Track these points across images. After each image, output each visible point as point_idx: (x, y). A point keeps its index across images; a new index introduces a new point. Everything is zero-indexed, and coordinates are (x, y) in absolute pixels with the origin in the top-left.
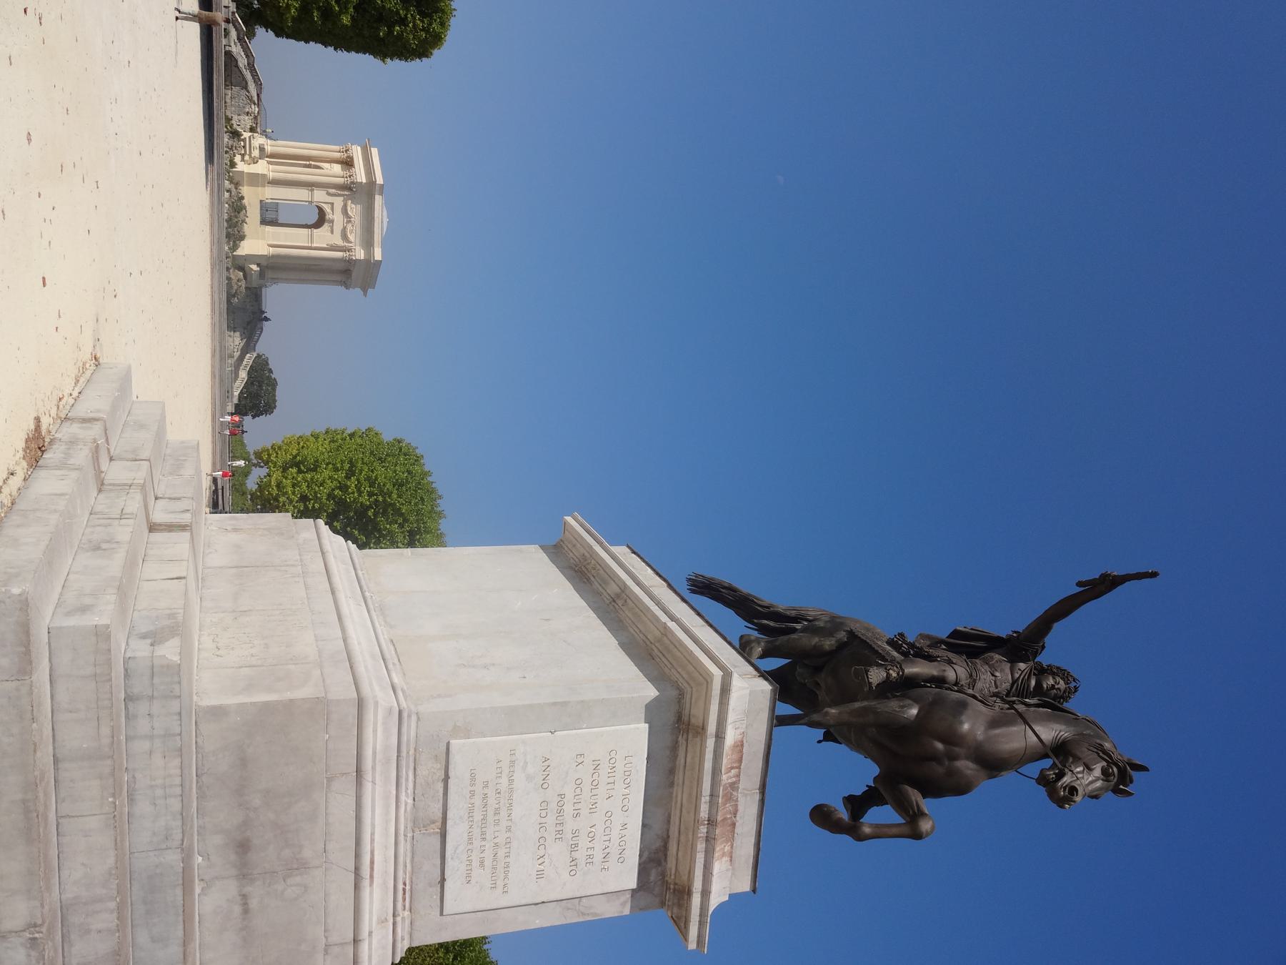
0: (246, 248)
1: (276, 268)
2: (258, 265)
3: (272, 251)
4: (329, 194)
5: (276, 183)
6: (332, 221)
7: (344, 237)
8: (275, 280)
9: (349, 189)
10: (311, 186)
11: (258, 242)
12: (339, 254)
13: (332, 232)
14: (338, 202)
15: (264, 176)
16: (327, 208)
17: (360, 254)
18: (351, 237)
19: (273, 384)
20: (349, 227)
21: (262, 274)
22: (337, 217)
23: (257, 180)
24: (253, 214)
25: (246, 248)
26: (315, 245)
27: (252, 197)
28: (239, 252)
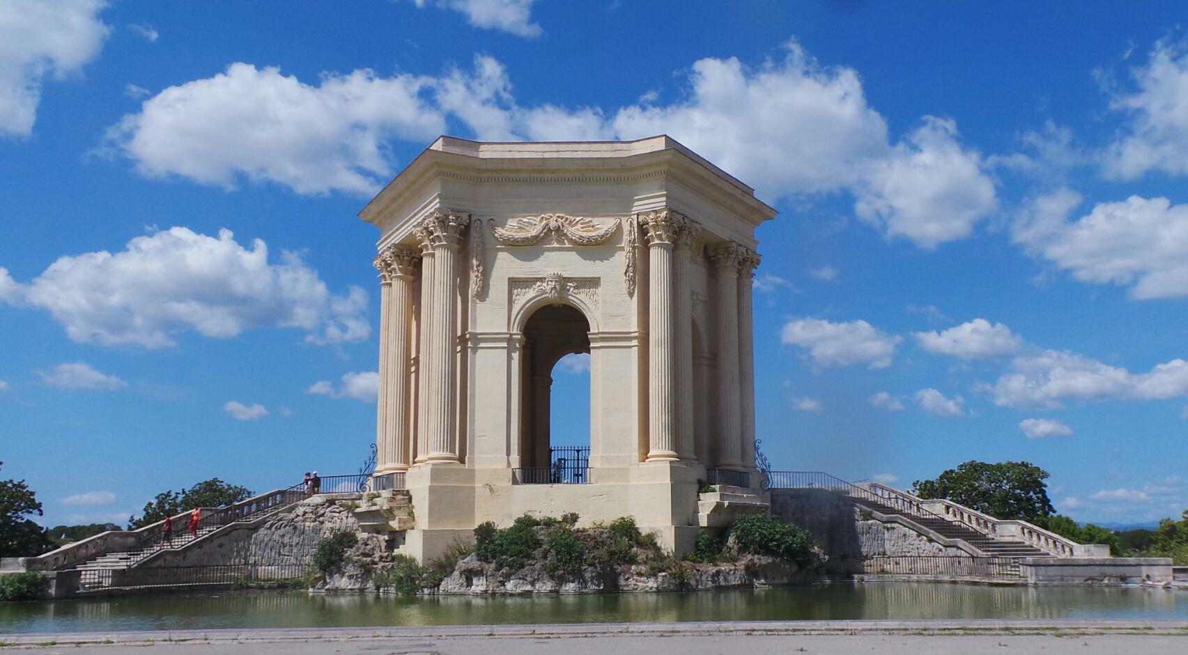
0: (656, 520)
1: (708, 438)
2: (703, 486)
3: (660, 447)
4: (483, 294)
6: (563, 281)
7: (599, 247)
8: (748, 446)
9: (468, 240)
10: (463, 343)
12: (658, 260)
13: (593, 283)
14: (506, 266)
15: (436, 473)
16: (525, 298)
18: (604, 225)
20: (577, 231)
21: (736, 479)
23: (451, 492)
24: (546, 502)
25: (656, 520)
26: (633, 326)
27: (509, 503)
28: (667, 542)
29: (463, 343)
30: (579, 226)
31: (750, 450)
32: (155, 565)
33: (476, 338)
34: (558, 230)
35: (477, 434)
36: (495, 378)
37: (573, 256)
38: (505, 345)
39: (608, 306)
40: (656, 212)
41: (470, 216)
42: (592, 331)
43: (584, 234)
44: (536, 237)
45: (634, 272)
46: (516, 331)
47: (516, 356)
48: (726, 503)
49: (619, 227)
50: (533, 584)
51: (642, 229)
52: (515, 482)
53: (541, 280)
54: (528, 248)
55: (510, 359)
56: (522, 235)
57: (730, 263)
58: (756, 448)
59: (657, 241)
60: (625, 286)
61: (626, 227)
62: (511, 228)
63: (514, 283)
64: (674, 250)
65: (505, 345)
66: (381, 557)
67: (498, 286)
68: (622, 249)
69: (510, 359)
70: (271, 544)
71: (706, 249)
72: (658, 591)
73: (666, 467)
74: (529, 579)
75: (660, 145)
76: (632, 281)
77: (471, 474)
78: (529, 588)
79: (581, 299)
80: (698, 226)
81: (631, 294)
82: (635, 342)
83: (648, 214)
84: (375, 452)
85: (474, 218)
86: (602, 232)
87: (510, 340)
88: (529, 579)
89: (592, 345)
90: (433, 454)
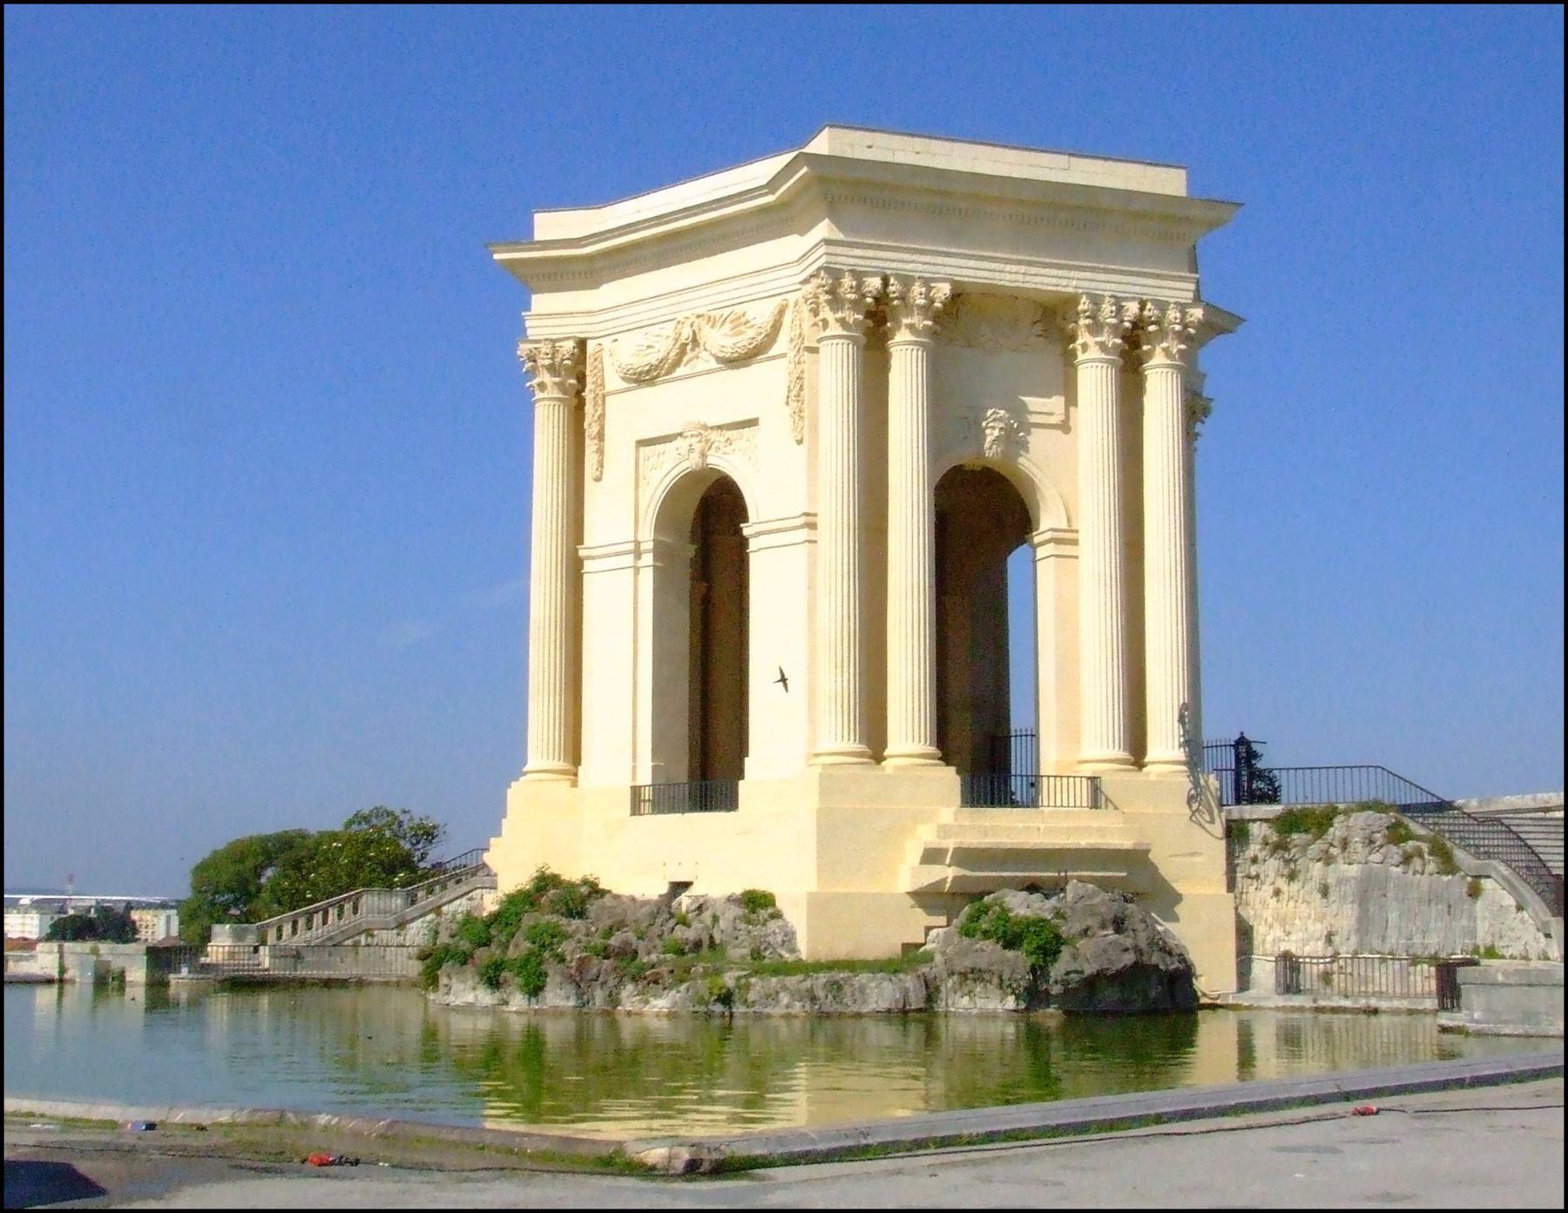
30: (728, 326)
46: (647, 536)
47: (647, 579)
52: (636, 810)
65: (629, 560)
68: (784, 355)
87: (638, 554)
89: (753, 544)
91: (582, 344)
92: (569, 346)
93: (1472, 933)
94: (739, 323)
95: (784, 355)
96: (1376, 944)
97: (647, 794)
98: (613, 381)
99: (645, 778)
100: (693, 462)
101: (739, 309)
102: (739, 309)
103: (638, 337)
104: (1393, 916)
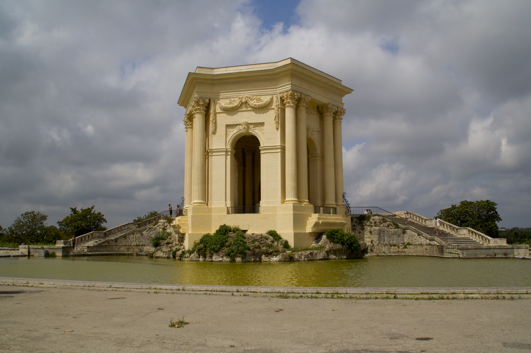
3: (291, 197)
4: (214, 133)
5: (205, 195)
6: (248, 124)
7: (263, 108)
10: (206, 153)
11: (278, 214)
12: (289, 113)
13: (262, 124)
16: (233, 133)
17: (285, 87)
18: (265, 99)
19: (465, 204)
20: (253, 103)
22: (245, 117)
26: (278, 143)
29: (206, 153)
30: (255, 100)
31: (340, 196)
32: (104, 245)
33: (212, 151)
34: (246, 102)
35: (213, 192)
36: (222, 169)
37: (252, 113)
38: (224, 153)
39: (268, 136)
40: (287, 92)
41: (210, 100)
42: (261, 146)
43: (257, 104)
44: (236, 107)
45: (278, 119)
47: (229, 158)
48: (321, 222)
49: (272, 100)
50: (222, 257)
51: (282, 100)
52: (228, 213)
53: (239, 125)
54: (230, 111)
55: (226, 158)
56: (231, 106)
57: (328, 114)
58: (344, 197)
59: (288, 105)
60: (274, 125)
61: (275, 99)
62: (223, 103)
63: (228, 126)
64: (297, 109)
65: (224, 153)
66: (176, 244)
67: (221, 129)
68: (273, 109)
69: (226, 158)
70: (148, 237)
71: (318, 107)
72: (279, 261)
73: (291, 205)
74: (221, 255)
75: (289, 61)
76: (277, 123)
77: (210, 210)
78: (221, 259)
79: (256, 132)
80: (309, 98)
81: (277, 129)
82: (279, 150)
83: (284, 93)
84: (183, 201)
85: (211, 100)
86: (264, 102)
87: (226, 152)
88: (221, 255)
89: (261, 152)
90: (195, 201)
91: (210, 100)
92: (207, 101)
93: (403, 240)
94: (259, 100)
95: (273, 109)
96: (382, 243)
97: (230, 210)
98: (218, 110)
99: (229, 205)
100: (244, 131)
101: (259, 97)
102: (259, 97)
103: (228, 101)
104: (386, 238)
